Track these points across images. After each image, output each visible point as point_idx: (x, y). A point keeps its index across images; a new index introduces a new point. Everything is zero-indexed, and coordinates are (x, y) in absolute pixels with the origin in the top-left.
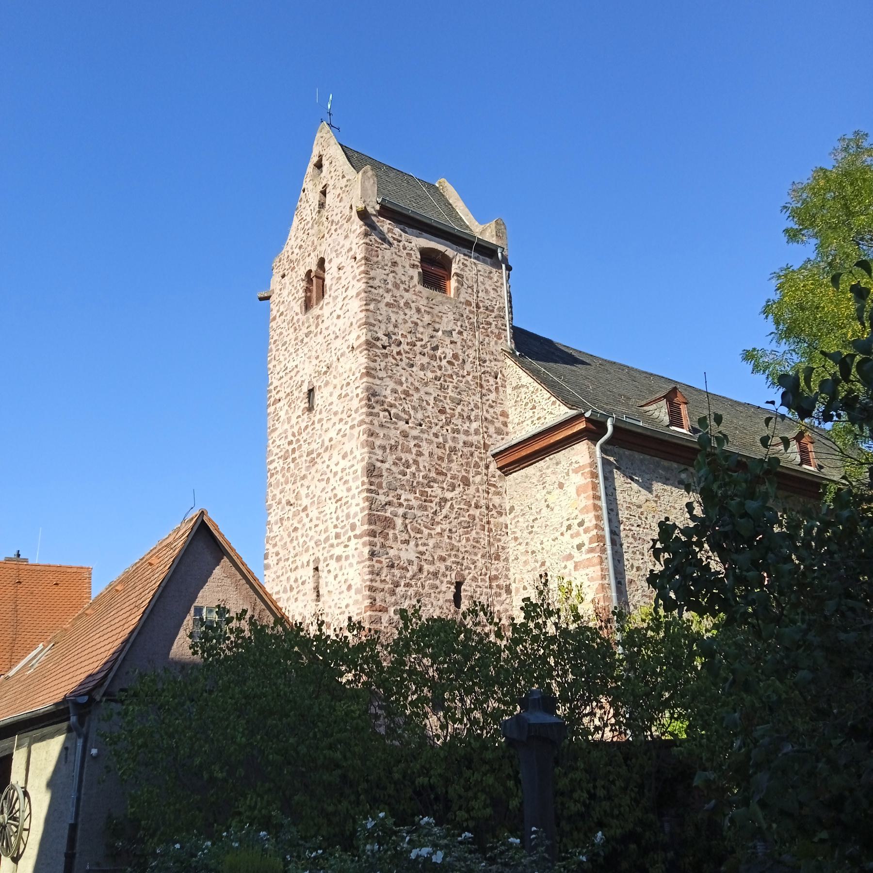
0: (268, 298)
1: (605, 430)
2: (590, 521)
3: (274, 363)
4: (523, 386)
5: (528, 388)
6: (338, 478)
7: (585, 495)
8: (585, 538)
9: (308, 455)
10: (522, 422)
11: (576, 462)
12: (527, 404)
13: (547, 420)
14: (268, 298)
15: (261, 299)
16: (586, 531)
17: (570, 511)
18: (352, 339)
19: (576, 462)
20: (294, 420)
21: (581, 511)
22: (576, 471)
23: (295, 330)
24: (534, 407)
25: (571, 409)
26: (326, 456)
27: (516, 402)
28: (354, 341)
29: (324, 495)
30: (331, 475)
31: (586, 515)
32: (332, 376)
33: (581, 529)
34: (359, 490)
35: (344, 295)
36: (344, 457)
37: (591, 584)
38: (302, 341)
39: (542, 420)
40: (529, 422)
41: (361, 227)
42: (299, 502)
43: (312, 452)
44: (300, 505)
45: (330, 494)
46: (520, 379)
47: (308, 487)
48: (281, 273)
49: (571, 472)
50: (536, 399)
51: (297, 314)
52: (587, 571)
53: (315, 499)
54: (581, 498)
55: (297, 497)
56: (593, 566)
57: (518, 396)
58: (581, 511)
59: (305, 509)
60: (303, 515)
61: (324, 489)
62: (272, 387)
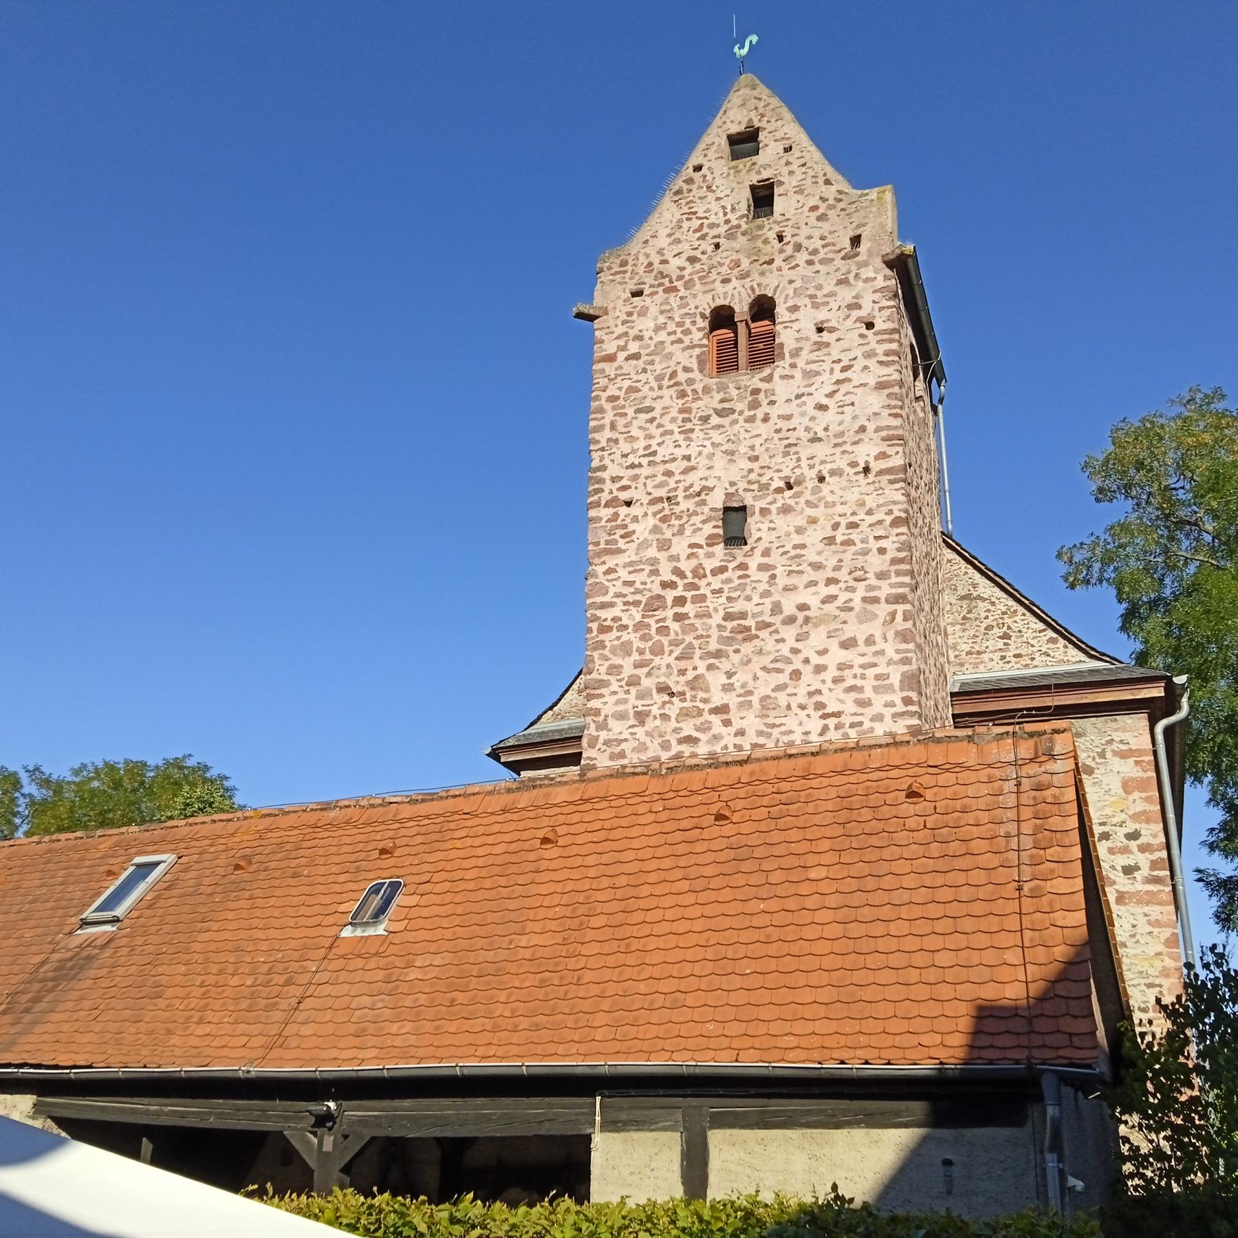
0: (592, 318)
1: (1180, 708)
2: (1155, 836)
3: (607, 433)
4: (979, 597)
5: (993, 604)
6: (828, 675)
7: (1144, 795)
8: (1143, 860)
9: (728, 617)
10: (979, 653)
11: (1121, 742)
13: (1035, 663)
14: (592, 318)
15: (580, 315)
16: (1143, 849)
17: (1108, 811)
18: (866, 451)
19: (1121, 742)
20: (680, 546)
21: (1135, 817)
22: (1123, 755)
23: (682, 394)
24: (1006, 636)
25: (1092, 657)
26: (789, 633)
27: (964, 618)
28: (871, 459)
29: (783, 699)
31: (1144, 825)
32: (802, 500)
33: (1133, 845)
34: (893, 710)
35: (838, 375)
36: (848, 644)
37: (1156, 931)
38: (705, 419)
41: (886, 278)
42: (701, 695)
43: (743, 615)
44: (705, 701)
45: (802, 699)
46: (975, 586)
47: (730, 675)
48: (632, 286)
49: (1109, 755)
50: (1013, 626)
51: (687, 369)
52: (1146, 909)
53: (755, 699)
54: (1131, 797)
55: (696, 683)
56: (1160, 904)
57: (970, 612)
58: (1135, 817)
59: (722, 709)
60: (716, 720)
61: (780, 688)
62: (605, 475)
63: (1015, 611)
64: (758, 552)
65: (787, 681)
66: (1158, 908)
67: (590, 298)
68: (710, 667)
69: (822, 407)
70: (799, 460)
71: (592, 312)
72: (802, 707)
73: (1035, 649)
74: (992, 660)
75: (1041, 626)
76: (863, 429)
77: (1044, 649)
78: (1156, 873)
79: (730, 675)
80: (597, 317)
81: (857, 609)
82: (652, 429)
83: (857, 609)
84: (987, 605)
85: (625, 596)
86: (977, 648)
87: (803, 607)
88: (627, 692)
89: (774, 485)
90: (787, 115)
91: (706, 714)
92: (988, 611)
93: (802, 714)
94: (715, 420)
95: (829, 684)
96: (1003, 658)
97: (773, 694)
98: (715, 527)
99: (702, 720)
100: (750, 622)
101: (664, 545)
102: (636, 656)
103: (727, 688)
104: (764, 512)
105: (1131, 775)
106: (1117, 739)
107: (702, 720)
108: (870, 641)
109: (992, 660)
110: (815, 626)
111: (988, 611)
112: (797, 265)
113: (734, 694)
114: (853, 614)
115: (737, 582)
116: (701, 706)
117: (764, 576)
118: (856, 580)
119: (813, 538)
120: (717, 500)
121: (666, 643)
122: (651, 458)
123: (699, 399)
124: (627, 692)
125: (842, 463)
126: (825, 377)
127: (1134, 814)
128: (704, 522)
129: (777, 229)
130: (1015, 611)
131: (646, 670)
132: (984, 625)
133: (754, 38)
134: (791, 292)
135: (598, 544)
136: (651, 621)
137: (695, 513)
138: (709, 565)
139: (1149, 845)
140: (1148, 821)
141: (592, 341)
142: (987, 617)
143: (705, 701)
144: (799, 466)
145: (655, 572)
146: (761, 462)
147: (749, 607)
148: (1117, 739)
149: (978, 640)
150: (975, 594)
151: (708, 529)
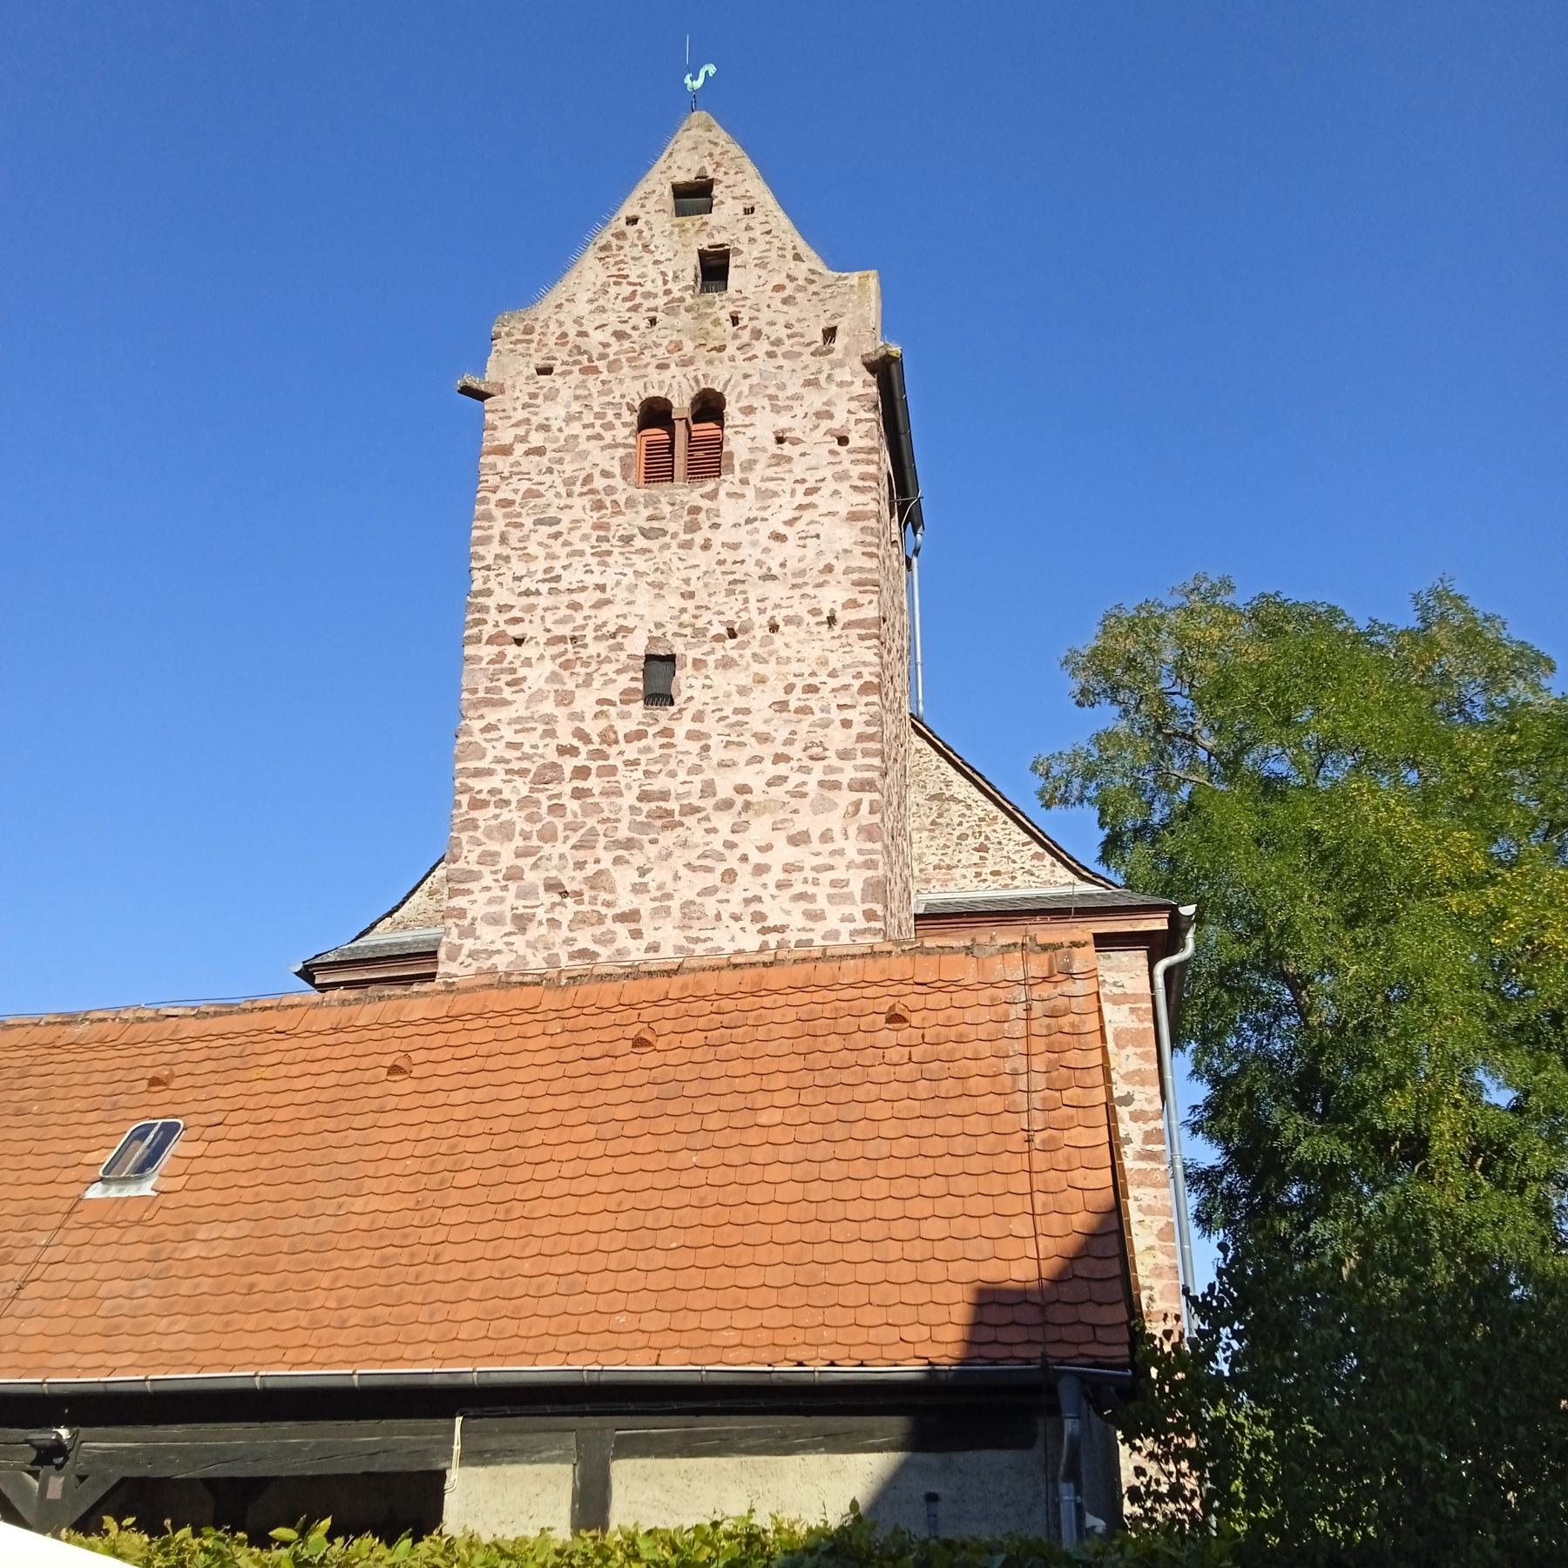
0: (482, 396)
1: (1184, 946)
2: (1150, 1101)
3: (495, 548)
4: (952, 798)
5: (969, 807)
6: (771, 878)
7: (1139, 1050)
9: (644, 796)
10: (949, 867)
11: (1115, 984)
12: (963, 837)
13: (1016, 883)
15: (467, 391)
18: (833, 597)
19: (1115, 984)
20: (585, 702)
23: (599, 506)
24: (982, 848)
25: (1084, 878)
26: (724, 821)
27: (933, 823)
28: (838, 608)
29: (711, 906)
30: (744, 871)
31: (1138, 1088)
32: (748, 653)
34: (852, 926)
35: (800, 499)
37: (1148, 1219)
38: (627, 540)
39: (1006, 880)
40: (970, 873)
42: (604, 896)
43: (664, 796)
44: (608, 904)
45: (735, 906)
46: (948, 784)
47: (643, 872)
50: (992, 836)
51: (606, 474)
53: (675, 905)
54: (1124, 1053)
55: (598, 881)
56: (1154, 1186)
57: (940, 816)
59: (631, 916)
60: (622, 930)
61: (708, 891)
62: (490, 602)
63: (995, 818)
64: (687, 715)
65: (718, 883)
66: (1151, 1191)
67: (481, 370)
68: (618, 861)
69: (779, 537)
70: (746, 601)
71: (483, 387)
72: (736, 918)
73: (1017, 866)
74: (965, 877)
75: (1025, 837)
76: (829, 569)
77: (1027, 867)
78: (1149, 1147)
79: (643, 872)
80: (489, 396)
81: (812, 795)
82: (556, 547)
83: (812, 795)
84: (961, 808)
85: (508, 761)
86: (947, 861)
87: (743, 789)
88: (505, 888)
89: (713, 631)
90: (750, 169)
91: (609, 921)
92: (963, 815)
93: (735, 926)
94: (640, 542)
95: (772, 890)
96: (978, 875)
97: (698, 900)
98: (633, 679)
99: (603, 928)
100: (673, 805)
101: (564, 699)
102: (518, 842)
103: (639, 889)
104: (698, 664)
105: (1125, 1025)
106: (1110, 980)
107: (603, 928)
108: (826, 837)
109: (965, 877)
110: (757, 814)
111: (963, 815)
112: (755, 357)
113: (647, 897)
114: (807, 801)
115: (658, 752)
116: (603, 910)
117: (694, 747)
118: (812, 758)
119: (760, 701)
120: (637, 645)
121: (560, 827)
122: (553, 585)
123: (620, 513)
124: (505, 888)
125: (801, 609)
126: (785, 499)
127: (1127, 1073)
128: (618, 672)
129: (731, 308)
130: (995, 818)
131: (531, 860)
132: (957, 833)
133: (711, 69)
134: (746, 390)
135: (475, 691)
136: (542, 797)
137: (608, 660)
138: (623, 727)
139: (1143, 1112)
140: (1143, 1083)
141: (481, 426)
142: (960, 824)
143: (608, 904)
144: (746, 609)
145: (549, 733)
146: (698, 601)
147: (673, 785)
148: (1110, 980)
149: (949, 851)
150: (948, 794)
151: (624, 682)
